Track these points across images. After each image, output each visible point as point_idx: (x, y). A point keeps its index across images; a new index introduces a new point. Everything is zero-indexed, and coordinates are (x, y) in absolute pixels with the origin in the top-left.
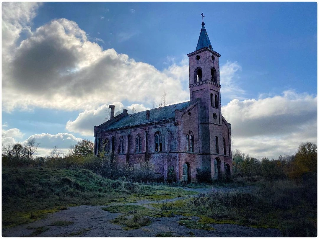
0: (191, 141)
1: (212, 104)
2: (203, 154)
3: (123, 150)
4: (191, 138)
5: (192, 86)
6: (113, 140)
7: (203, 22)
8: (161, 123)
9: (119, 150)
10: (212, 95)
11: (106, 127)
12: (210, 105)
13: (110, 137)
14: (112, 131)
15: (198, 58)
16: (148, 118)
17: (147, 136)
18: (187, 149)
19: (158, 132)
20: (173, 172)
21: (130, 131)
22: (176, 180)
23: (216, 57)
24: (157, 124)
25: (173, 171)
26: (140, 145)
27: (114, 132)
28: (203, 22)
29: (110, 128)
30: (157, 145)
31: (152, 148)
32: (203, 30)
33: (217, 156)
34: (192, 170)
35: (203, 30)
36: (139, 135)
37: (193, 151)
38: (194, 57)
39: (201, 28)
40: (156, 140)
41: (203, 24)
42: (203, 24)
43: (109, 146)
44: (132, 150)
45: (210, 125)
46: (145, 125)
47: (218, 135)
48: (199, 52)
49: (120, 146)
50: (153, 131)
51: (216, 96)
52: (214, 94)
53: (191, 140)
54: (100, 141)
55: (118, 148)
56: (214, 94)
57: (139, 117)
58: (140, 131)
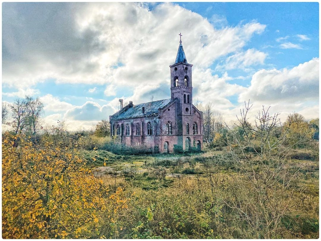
0: (170, 128)
1: (185, 102)
2: (178, 135)
3: (129, 133)
4: (170, 125)
5: (172, 89)
6: (122, 126)
7: (181, 40)
8: (151, 117)
9: (126, 133)
10: (185, 95)
11: (117, 116)
12: (183, 102)
13: (120, 124)
14: (121, 120)
15: (176, 69)
16: (143, 113)
17: (142, 125)
18: (167, 133)
19: (149, 123)
20: (158, 148)
21: (132, 120)
22: (159, 152)
23: (189, 67)
24: (149, 117)
25: (158, 147)
26: (139, 130)
27: (122, 121)
28: (181, 40)
29: (120, 117)
30: (149, 130)
31: (146, 133)
32: (181, 47)
33: (188, 136)
34: (170, 146)
35: (181, 47)
36: (138, 123)
37: (172, 133)
38: (174, 68)
39: (179, 45)
40: (148, 127)
41: (181, 42)
42: (181, 42)
43: (120, 131)
44: (135, 134)
45: (183, 116)
46: (141, 117)
47: (189, 123)
48: (177, 65)
49: (126, 130)
50: (146, 121)
51: (188, 96)
52: (187, 94)
53: (171, 126)
54: (113, 127)
55: (125, 132)
56: (187, 94)
57: (139, 109)
58: (139, 121)
